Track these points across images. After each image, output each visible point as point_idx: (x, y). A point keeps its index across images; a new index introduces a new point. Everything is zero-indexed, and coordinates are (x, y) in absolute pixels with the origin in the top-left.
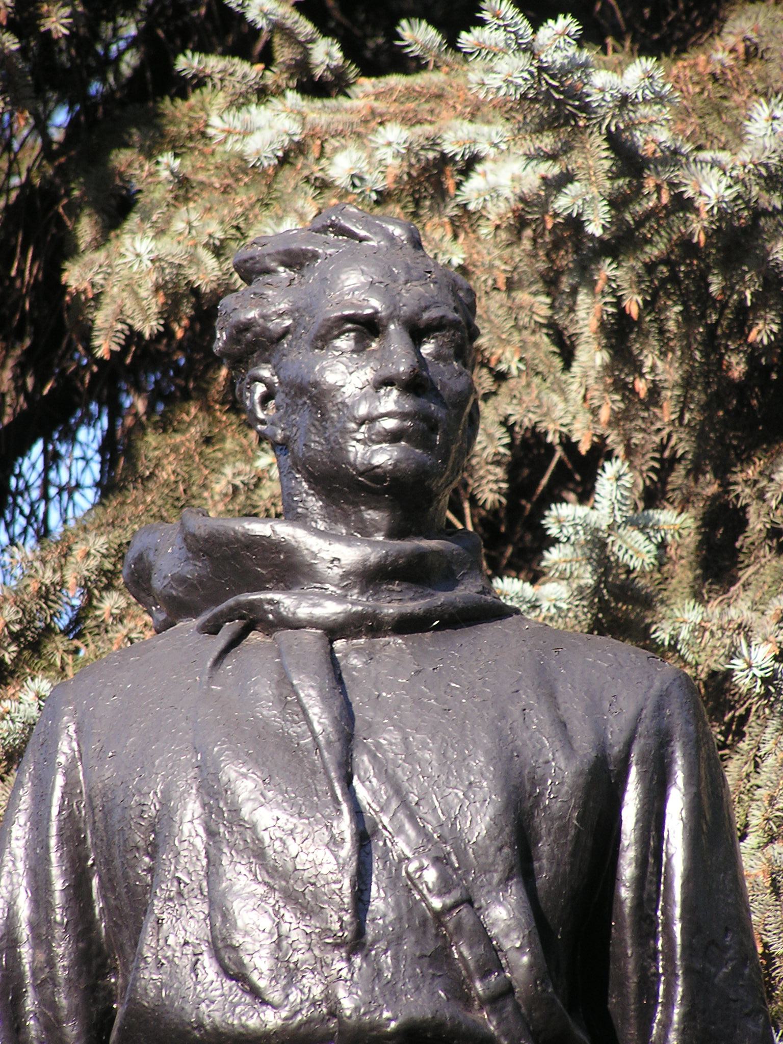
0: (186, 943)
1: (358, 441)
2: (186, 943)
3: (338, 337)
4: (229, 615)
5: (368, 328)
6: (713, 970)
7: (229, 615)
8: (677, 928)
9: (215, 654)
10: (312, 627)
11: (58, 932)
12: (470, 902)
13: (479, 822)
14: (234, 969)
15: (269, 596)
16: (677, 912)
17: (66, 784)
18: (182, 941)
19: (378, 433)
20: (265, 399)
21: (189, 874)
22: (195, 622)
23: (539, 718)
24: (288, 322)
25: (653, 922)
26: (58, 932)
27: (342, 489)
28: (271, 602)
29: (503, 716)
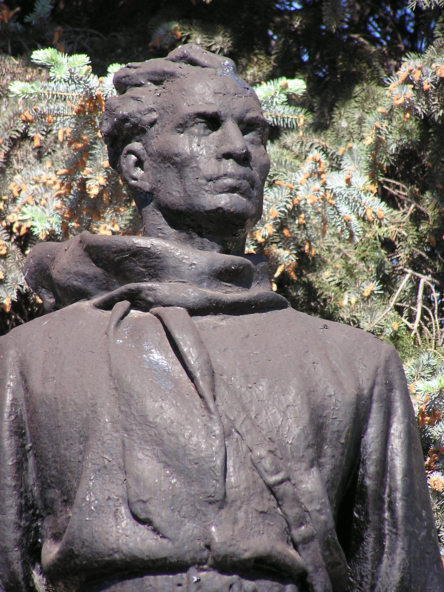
0: (109, 498)
1: (207, 191)
2: (109, 498)
3: (193, 126)
4: (121, 297)
5: (213, 121)
6: (417, 532)
7: (121, 297)
8: (399, 505)
9: (171, 308)
10: (178, 306)
11: (8, 492)
12: (289, 479)
13: (294, 430)
14: (143, 516)
15: (149, 285)
16: (399, 495)
17: (13, 399)
18: (107, 498)
19: (221, 187)
20: (139, 163)
21: (112, 454)
22: (85, 304)
23: (320, 369)
24: (154, 116)
25: (382, 501)
26: (8, 492)
27: (190, 222)
28: (151, 289)
29: (301, 367)
